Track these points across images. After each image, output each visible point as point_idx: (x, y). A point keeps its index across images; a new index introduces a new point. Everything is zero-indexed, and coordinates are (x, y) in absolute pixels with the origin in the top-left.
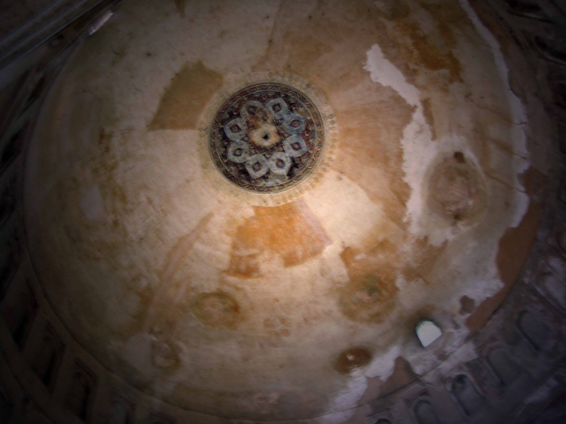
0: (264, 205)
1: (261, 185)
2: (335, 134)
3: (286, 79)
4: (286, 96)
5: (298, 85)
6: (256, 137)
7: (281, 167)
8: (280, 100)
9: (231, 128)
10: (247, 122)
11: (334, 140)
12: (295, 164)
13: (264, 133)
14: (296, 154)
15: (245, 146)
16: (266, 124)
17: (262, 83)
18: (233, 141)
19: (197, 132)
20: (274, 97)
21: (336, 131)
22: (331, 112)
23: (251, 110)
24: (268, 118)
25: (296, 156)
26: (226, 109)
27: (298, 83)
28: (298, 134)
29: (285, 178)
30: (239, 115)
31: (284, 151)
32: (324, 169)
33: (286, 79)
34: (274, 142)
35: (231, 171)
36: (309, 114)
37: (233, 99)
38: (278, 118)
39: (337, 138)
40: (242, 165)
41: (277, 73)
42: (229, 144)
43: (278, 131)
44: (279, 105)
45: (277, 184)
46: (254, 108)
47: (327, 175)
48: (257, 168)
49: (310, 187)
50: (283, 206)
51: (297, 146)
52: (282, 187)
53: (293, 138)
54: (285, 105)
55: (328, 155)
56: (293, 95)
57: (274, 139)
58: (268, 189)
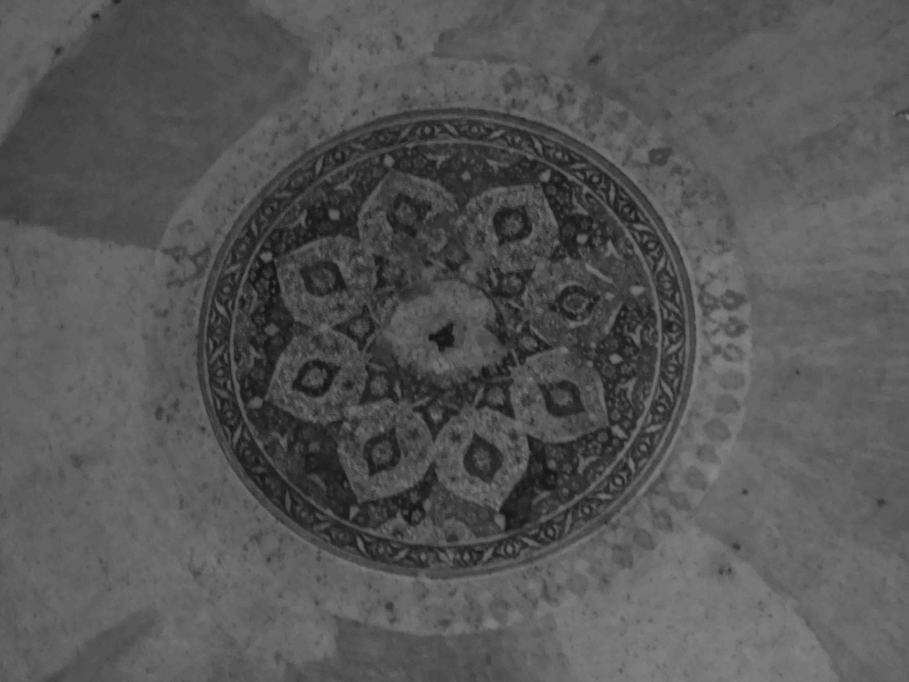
0: (381, 619)
1: (386, 531)
2: (737, 380)
3: (573, 113)
4: (559, 182)
5: (616, 146)
6: (405, 329)
7: (487, 476)
8: (525, 195)
9: (305, 272)
10: (380, 261)
11: (728, 405)
12: (543, 472)
13: (440, 318)
14: (555, 431)
15: (350, 360)
16: (457, 284)
17: (471, 111)
18: (304, 329)
19: (162, 262)
20: (509, 178)
21: (745, 368)
22: (737, 286)
23: (404, 213)
24: (467, 258)
25: (556, 441)
26: (300, 189)
27: (620, 139)
28: (580, 350)
29: (491, 519)
30: (347, 225)
31: (507, 409)
32: (665, 514)
33: (573, 113)
34: (469, 366)
35: (272, 447)
36: (641, 275)
37: (337, 152)
38: (508, 266)
39: (740, 395)
40: (324, 433)
41: (542, 81)
42: (285, 337)
43: (500, 319)
44: (522, 213)
45: (452, 538)
46: (421, 208)
47: (669, 542)
48: (386, 458)
49: (593, 580)
50: (462, 637)
51: (564, 399)
52: (471, 558)
53: (557, 363)
54: (546, 219)
55: (688, 460)
56: (588, 182)
57: (473, 353)
58: (415, 559)
